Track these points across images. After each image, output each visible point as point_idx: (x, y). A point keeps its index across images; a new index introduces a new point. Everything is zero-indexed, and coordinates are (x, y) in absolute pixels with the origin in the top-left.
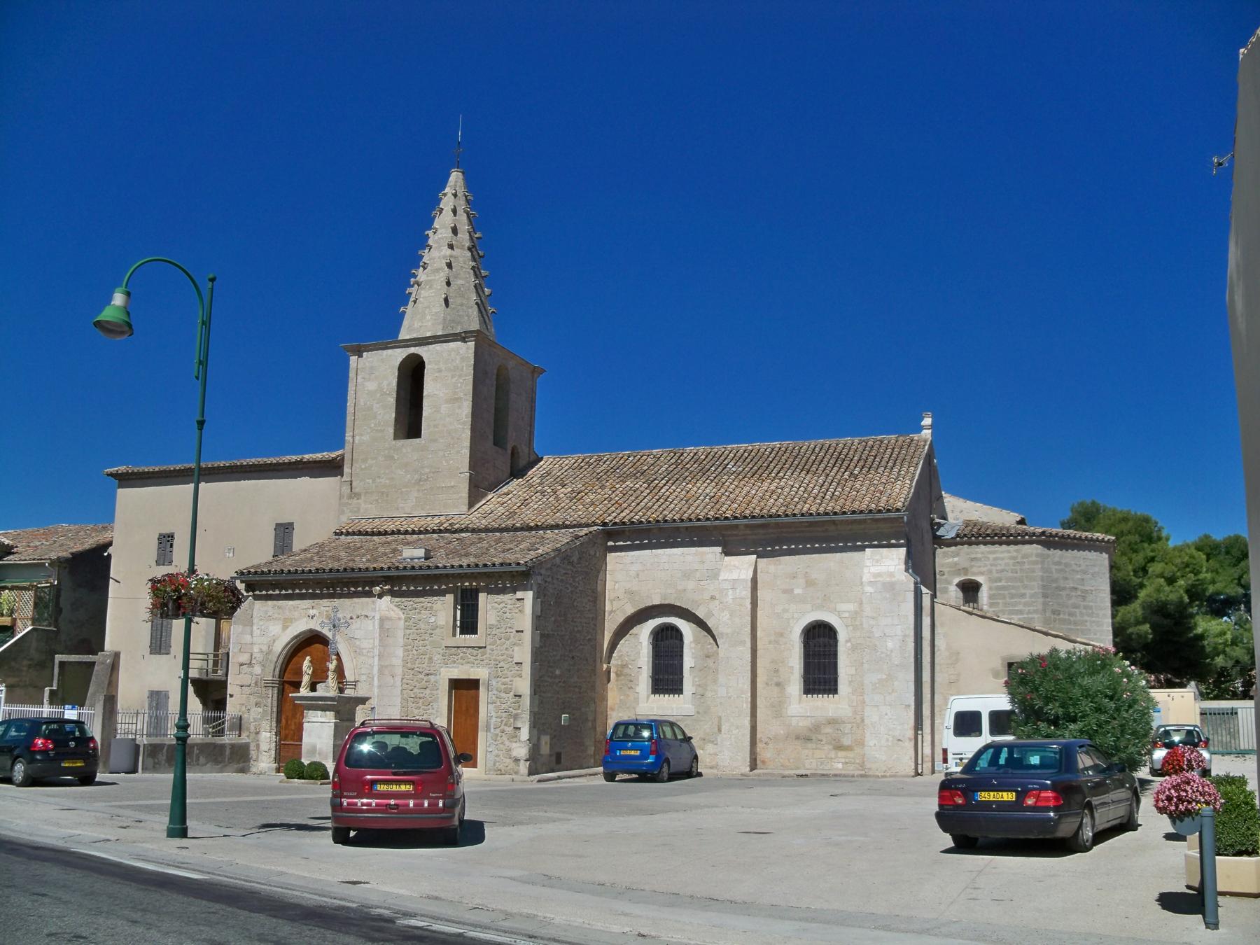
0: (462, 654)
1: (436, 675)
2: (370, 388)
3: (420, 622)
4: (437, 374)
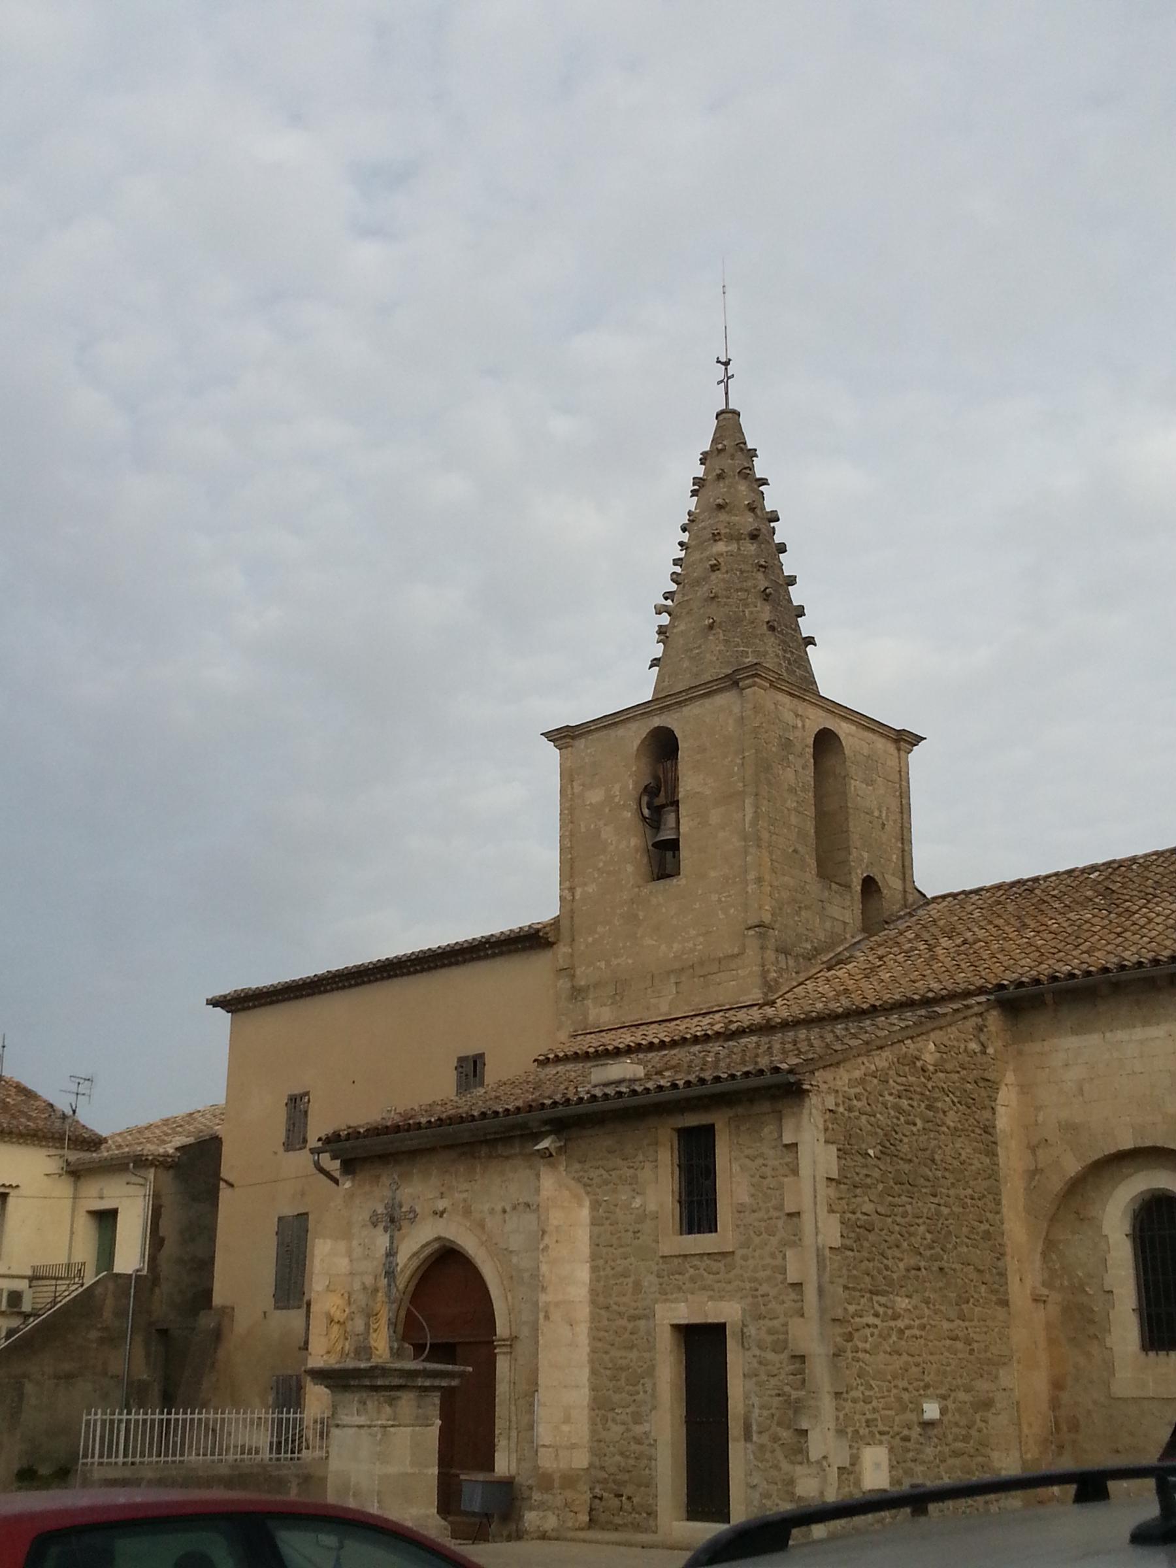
0: (692, 1271)
2: (593, 801)
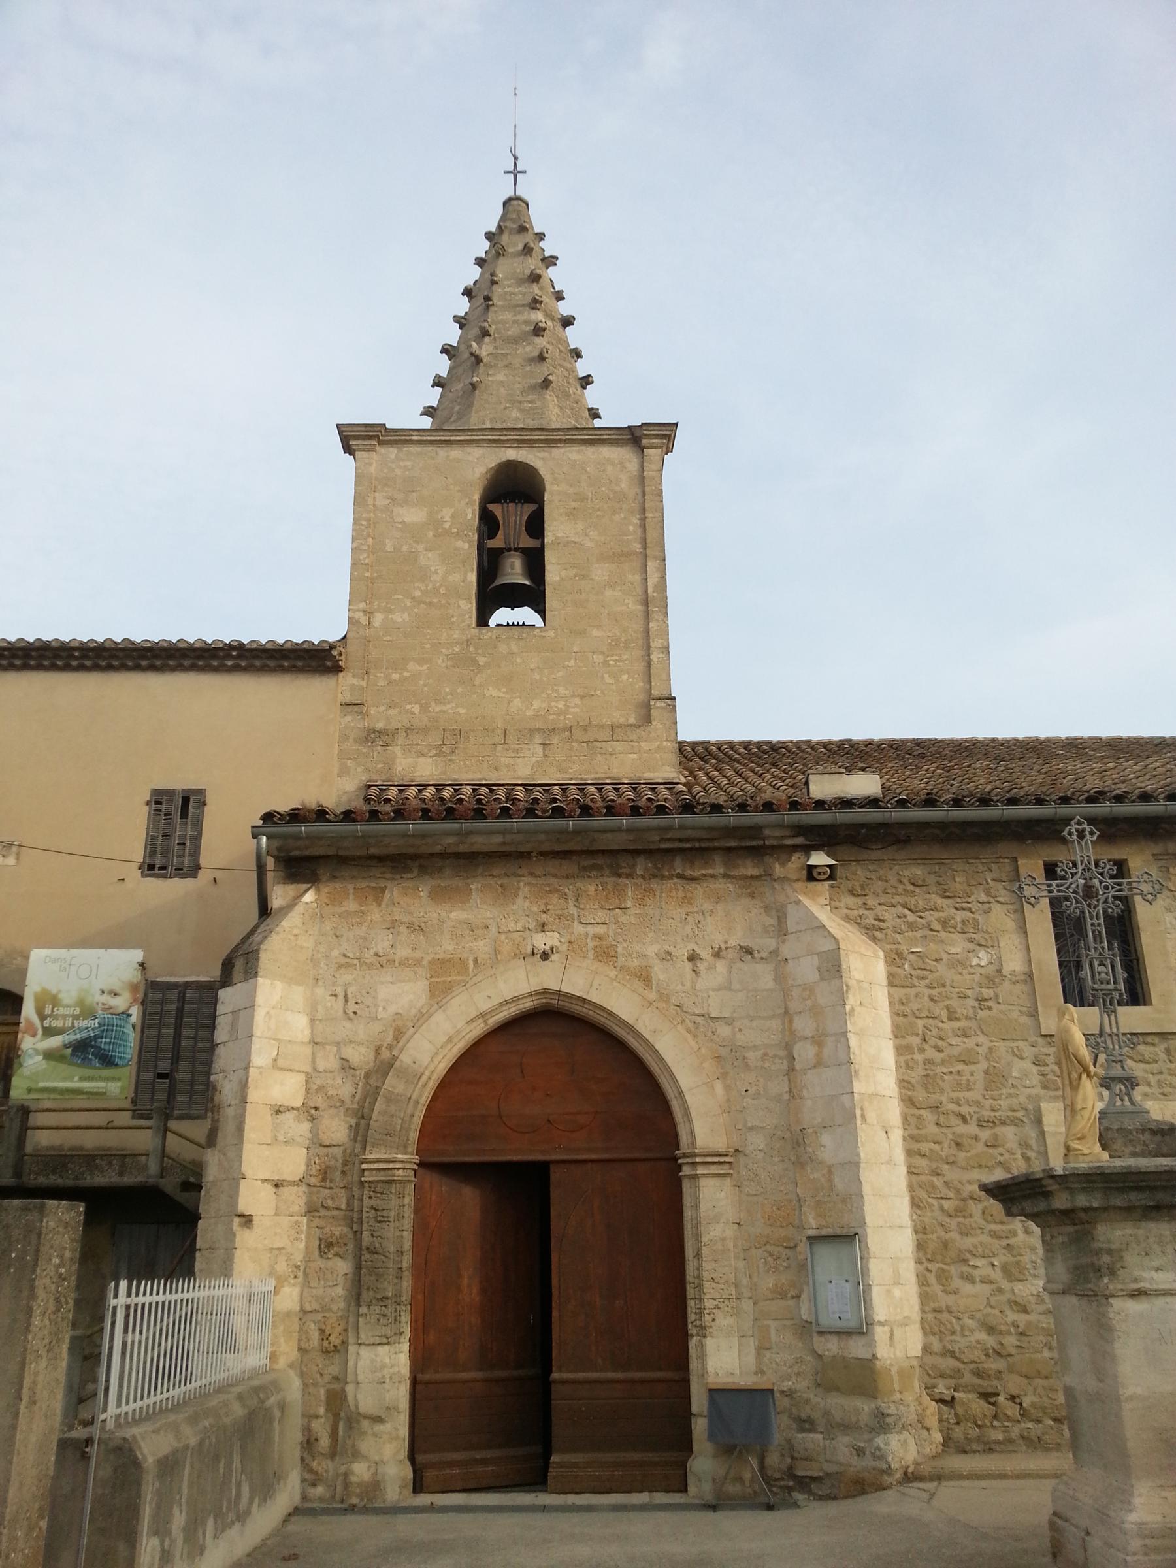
1: (1017, 1122)
3: (941, 968)
4: (574, 504)
